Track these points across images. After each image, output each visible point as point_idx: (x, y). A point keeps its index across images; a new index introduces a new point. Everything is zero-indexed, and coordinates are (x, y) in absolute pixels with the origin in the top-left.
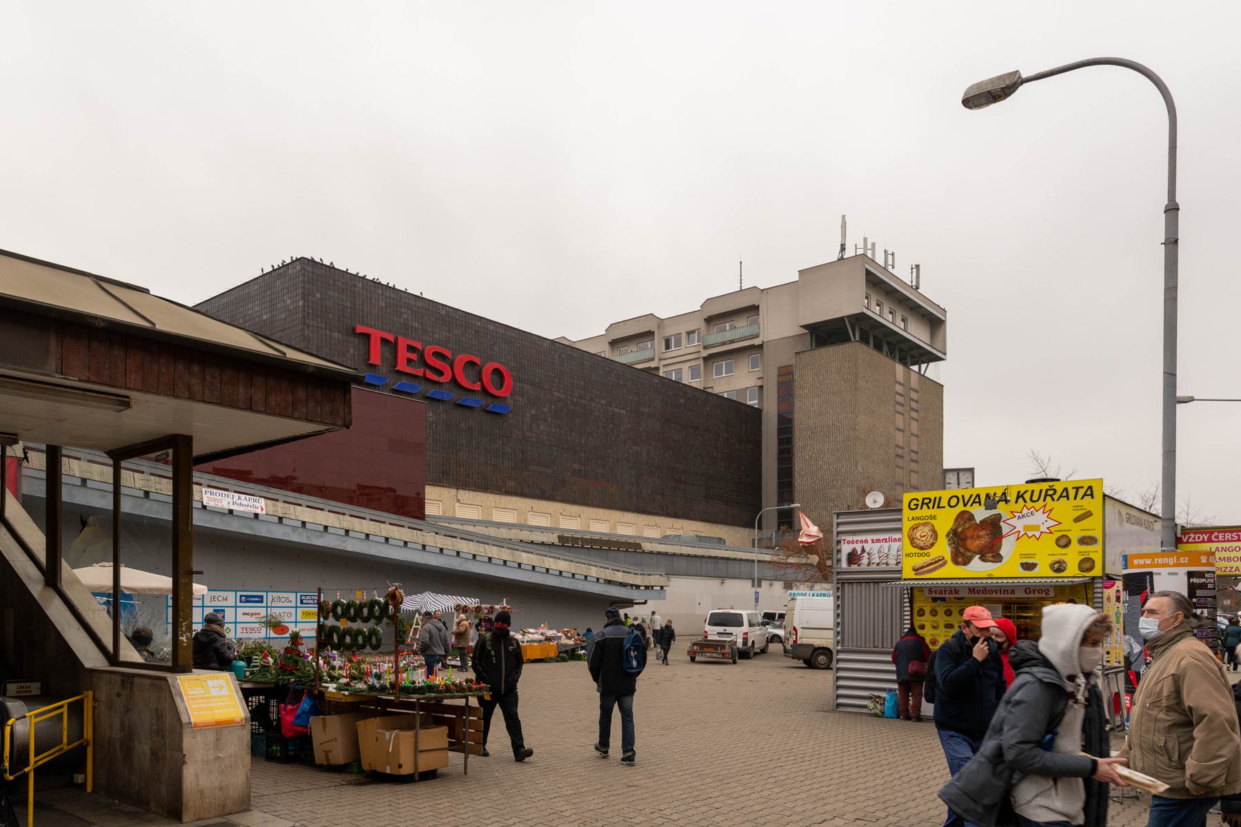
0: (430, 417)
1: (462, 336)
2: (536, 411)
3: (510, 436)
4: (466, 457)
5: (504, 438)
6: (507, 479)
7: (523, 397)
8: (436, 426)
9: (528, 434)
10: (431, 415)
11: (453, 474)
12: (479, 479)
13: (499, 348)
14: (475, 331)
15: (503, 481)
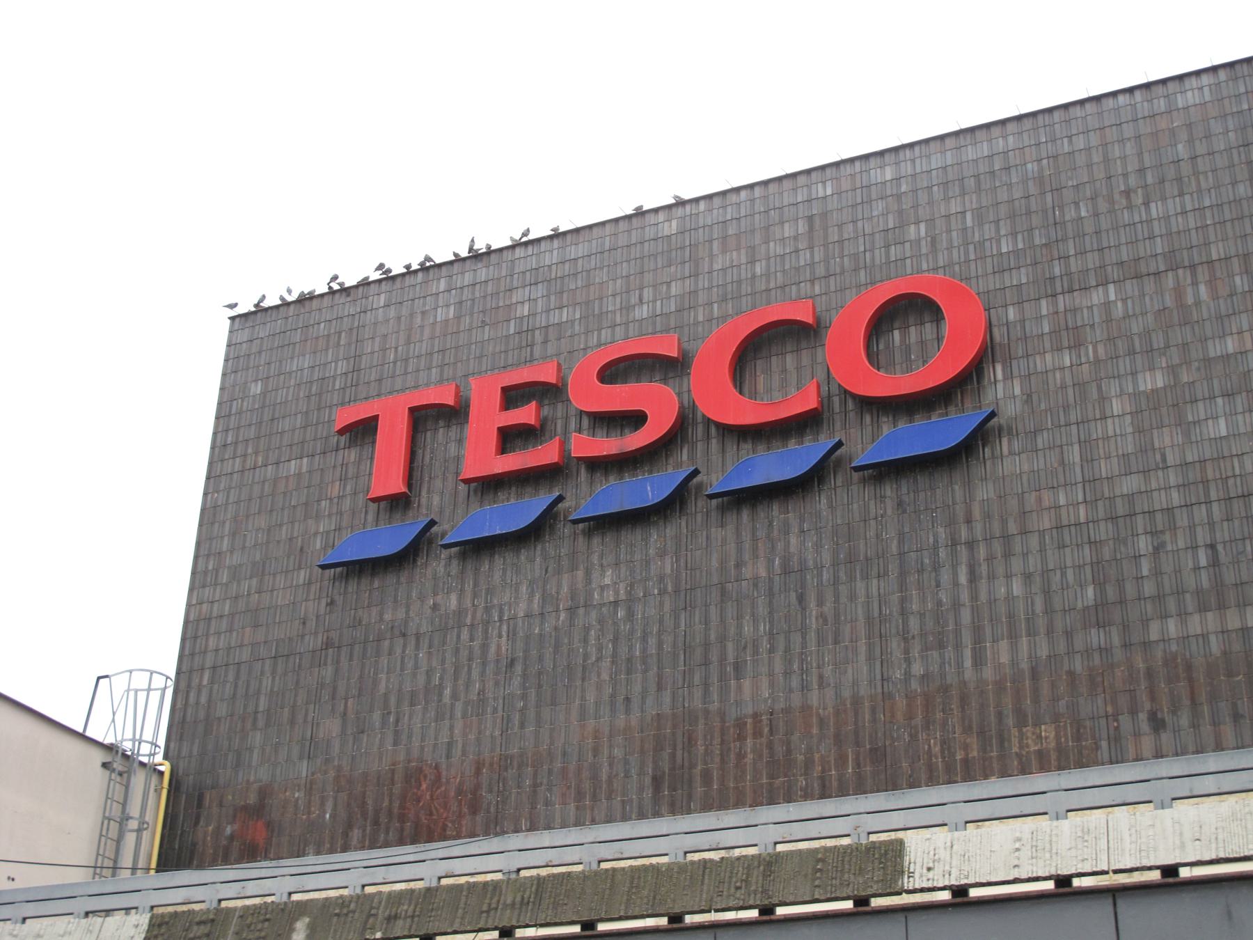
0: (602, 588)
1: (752, 262)
2: (1172, 370)
3: (1013, 528)
4: (772, 685)
5: (982, 552)
6: (1010, 721)
7: (1077, 345)
8: (630, 615)
9: (1130, 484)
10: (607, 581)
11: (707, 777)
12: (842, 760)
13: (931, 222)
14: (810, 219)
15: (982, 733)
